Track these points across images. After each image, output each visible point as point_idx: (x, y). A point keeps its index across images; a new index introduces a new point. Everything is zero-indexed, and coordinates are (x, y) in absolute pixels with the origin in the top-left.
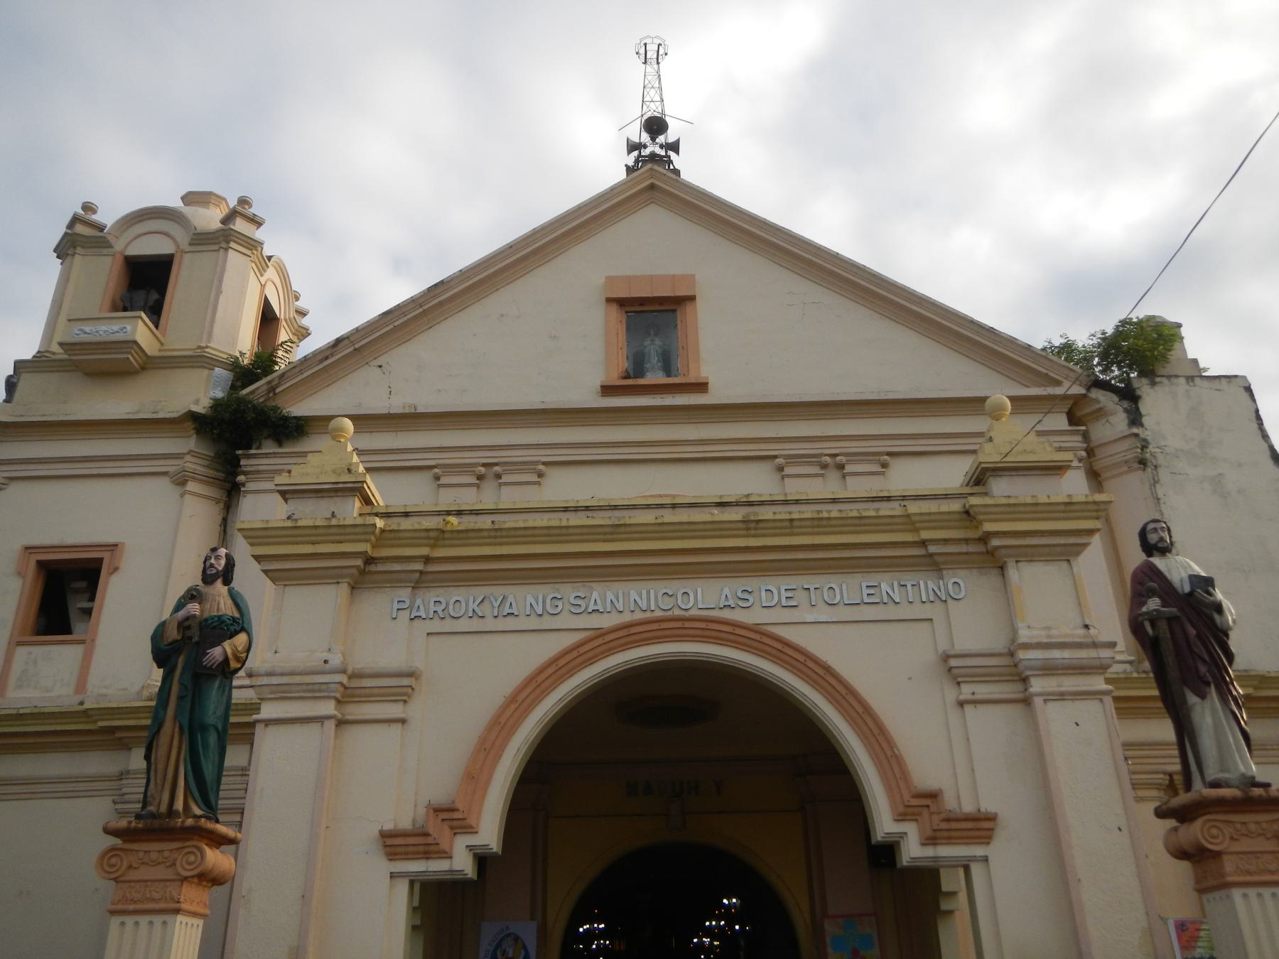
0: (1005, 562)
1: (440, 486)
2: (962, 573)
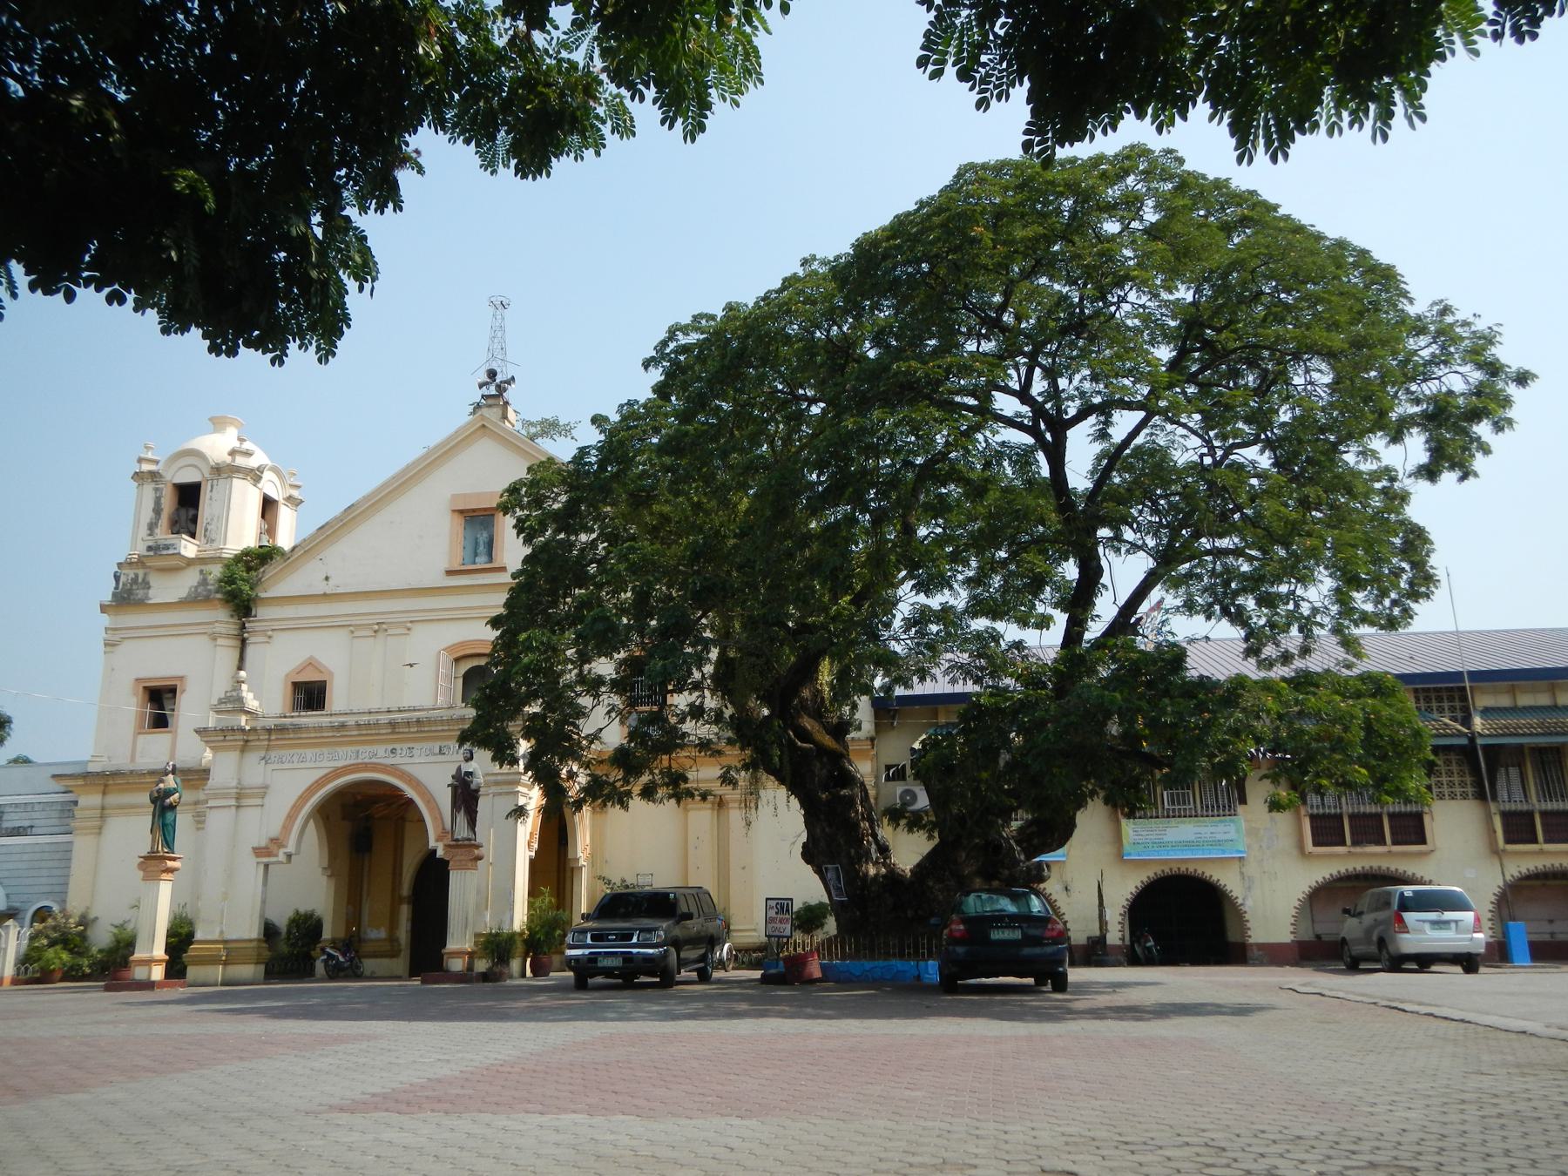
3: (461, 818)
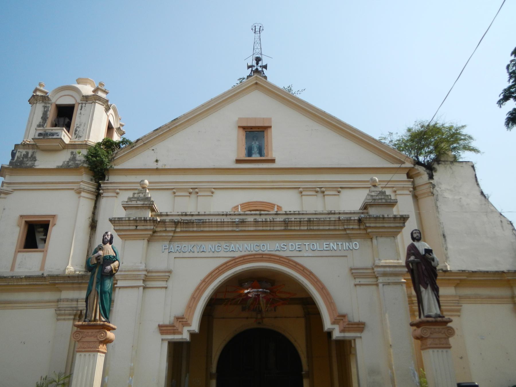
0: (372, 237)
1: (175, 196)
2: (358, 240)
3: (427, 294)
